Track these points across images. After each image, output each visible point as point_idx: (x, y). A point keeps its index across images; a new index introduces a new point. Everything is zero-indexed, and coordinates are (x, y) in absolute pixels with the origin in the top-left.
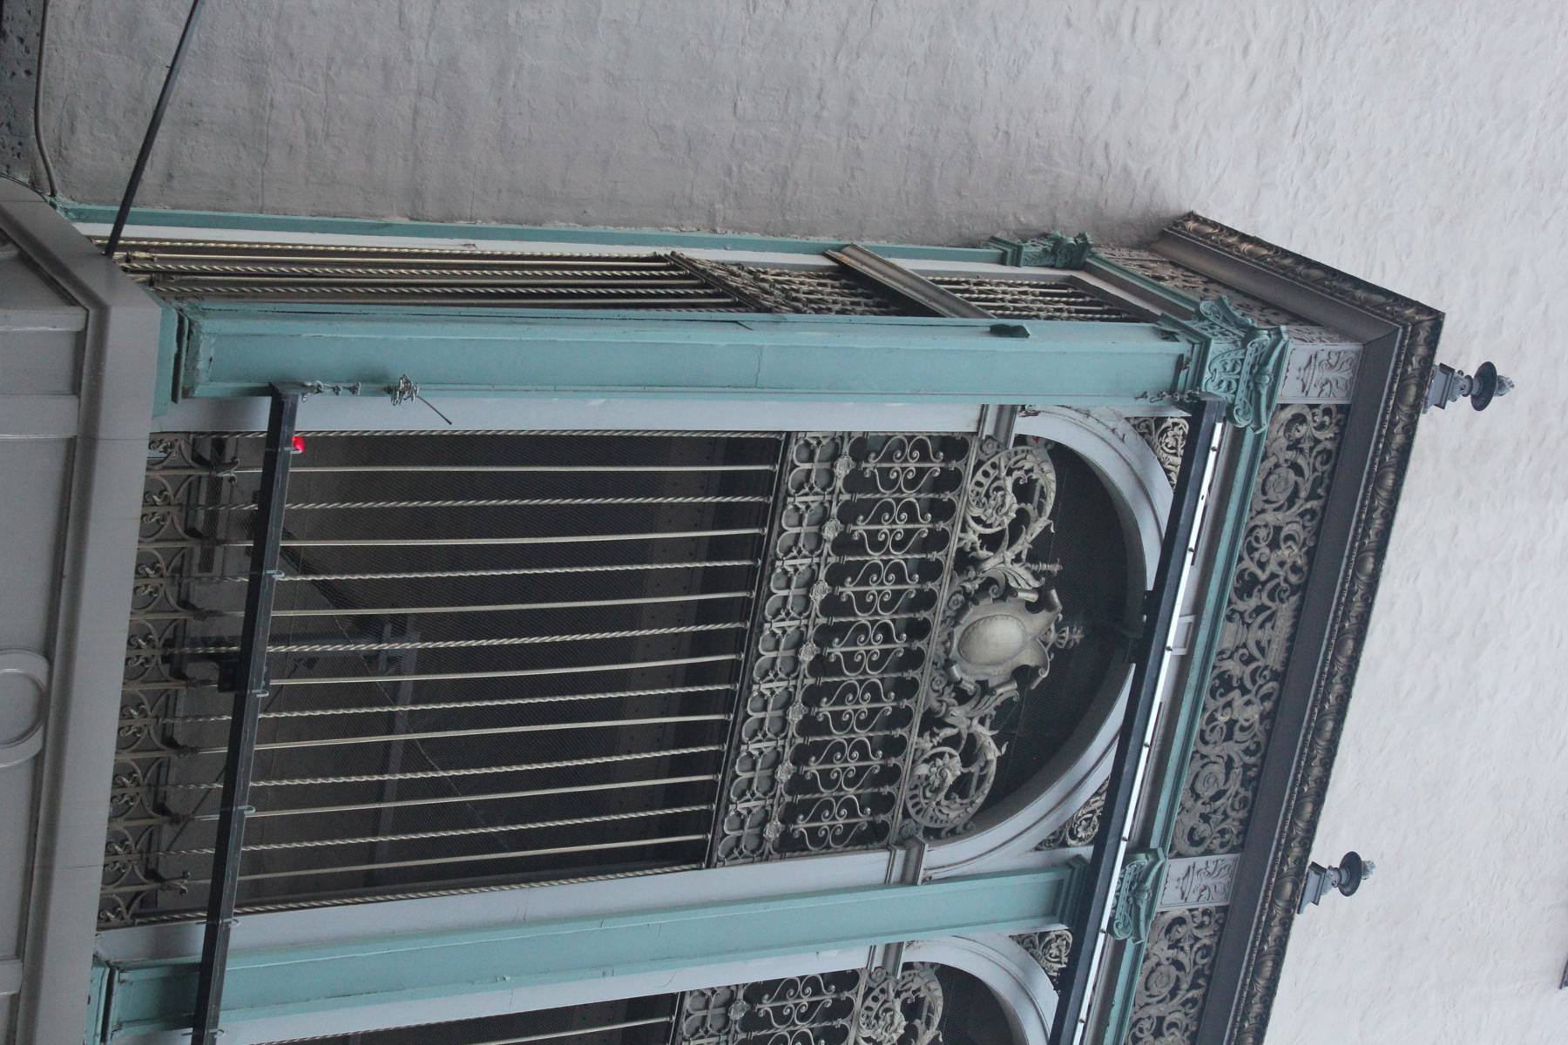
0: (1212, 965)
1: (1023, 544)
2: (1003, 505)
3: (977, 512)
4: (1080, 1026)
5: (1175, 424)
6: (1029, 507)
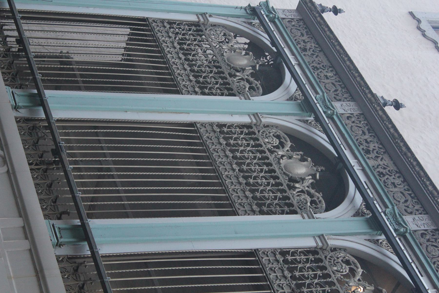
0: (404, 178)
1: (358, 277)
2: (342, 266)
3: (335, 268)
4: (413, 264)
5: (383, 241)
6: (351, 266)
